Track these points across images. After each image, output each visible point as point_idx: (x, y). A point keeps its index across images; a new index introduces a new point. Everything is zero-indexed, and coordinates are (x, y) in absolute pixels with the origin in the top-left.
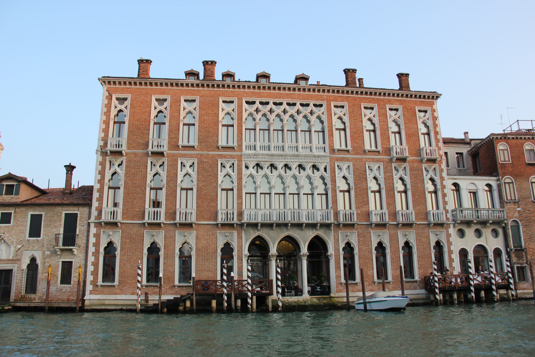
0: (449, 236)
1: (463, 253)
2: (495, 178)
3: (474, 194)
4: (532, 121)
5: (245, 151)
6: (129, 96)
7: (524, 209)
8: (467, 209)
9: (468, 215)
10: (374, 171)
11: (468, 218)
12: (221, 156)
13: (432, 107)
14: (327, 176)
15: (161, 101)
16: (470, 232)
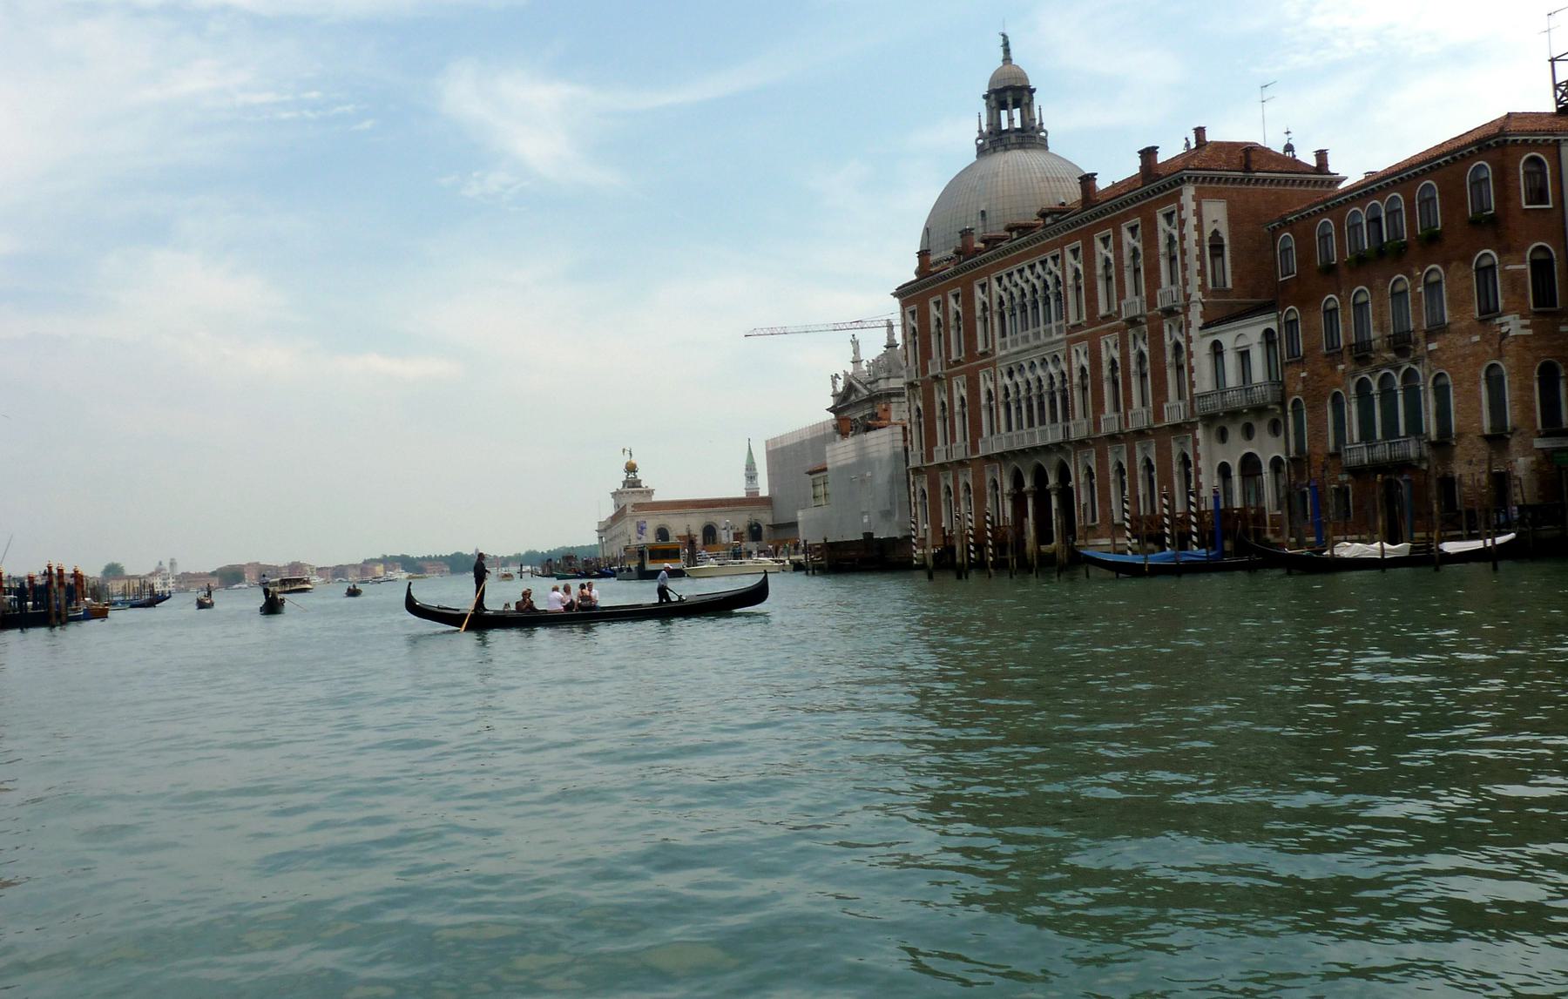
0: (1196, 442)
1: (1224, 470)
2: (1274, 315)
3: (1244, 355)
4: (1553, 60)
5: (1000, 353)
6: (914, 307)
7: (1312, 373)
8: (1233, 389)
9: (1235, 400)
10: (1109, 351)
11: (1258, 401)
12: (983, 366)
13: (1178, 200)
14: (1064, 367)
15: (937, 304)
16: (1235, 434)
